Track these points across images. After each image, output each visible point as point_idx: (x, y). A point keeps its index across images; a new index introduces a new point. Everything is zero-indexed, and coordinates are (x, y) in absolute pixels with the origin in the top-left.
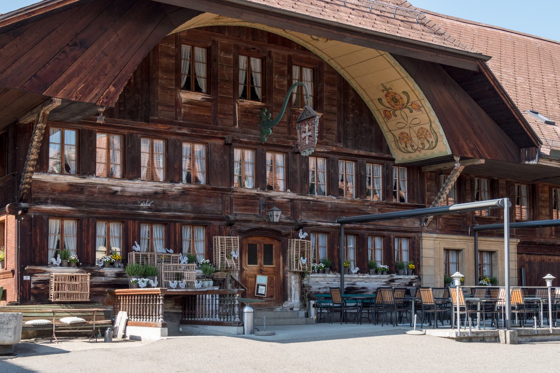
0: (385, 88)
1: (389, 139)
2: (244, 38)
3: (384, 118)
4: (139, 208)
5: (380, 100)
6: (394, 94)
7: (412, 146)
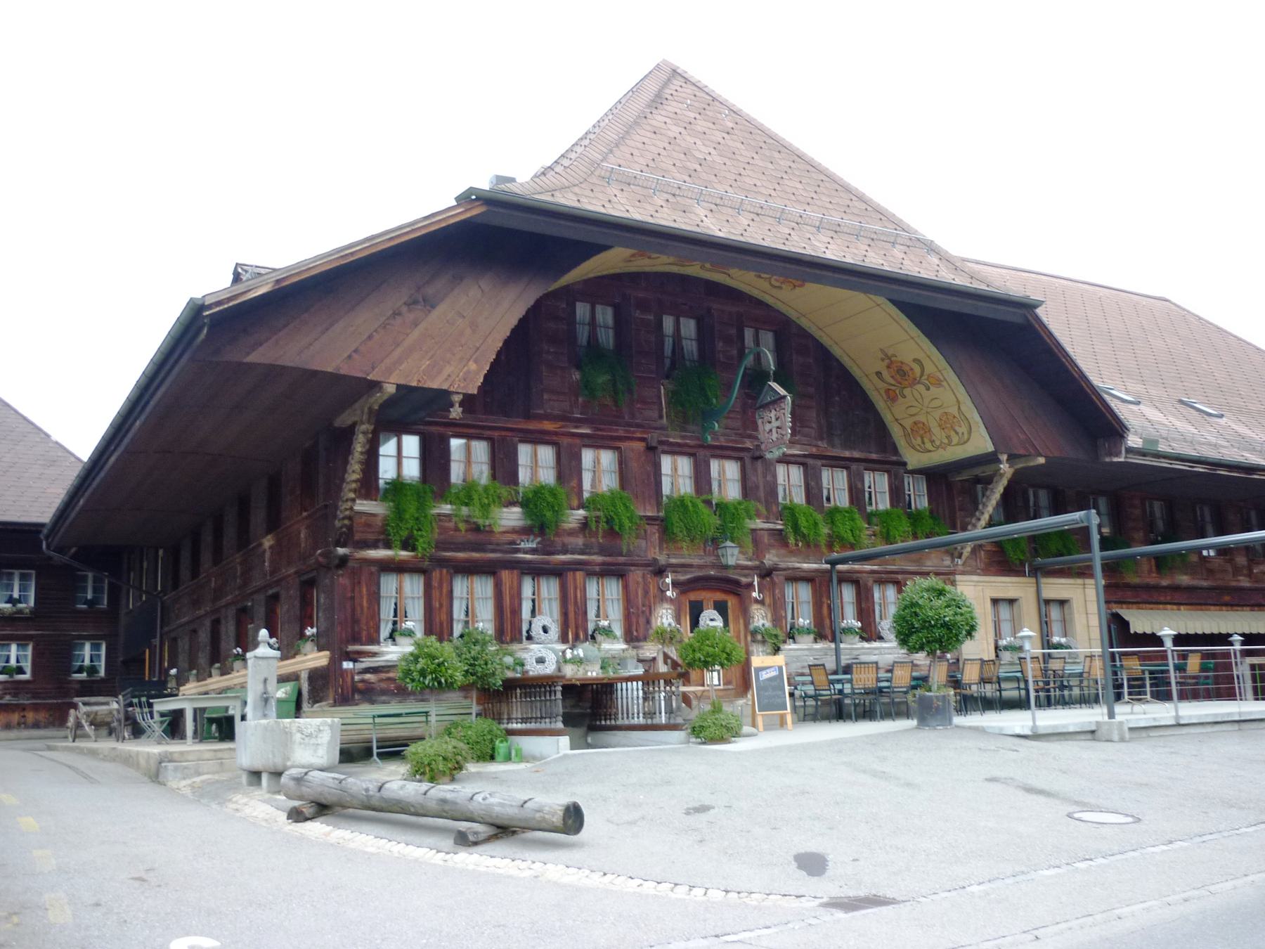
0: (886, 355)
1: (896, 432)
4: (518, 551)
5: (879, 374)
6: (899, 364)
7: (932, 442)
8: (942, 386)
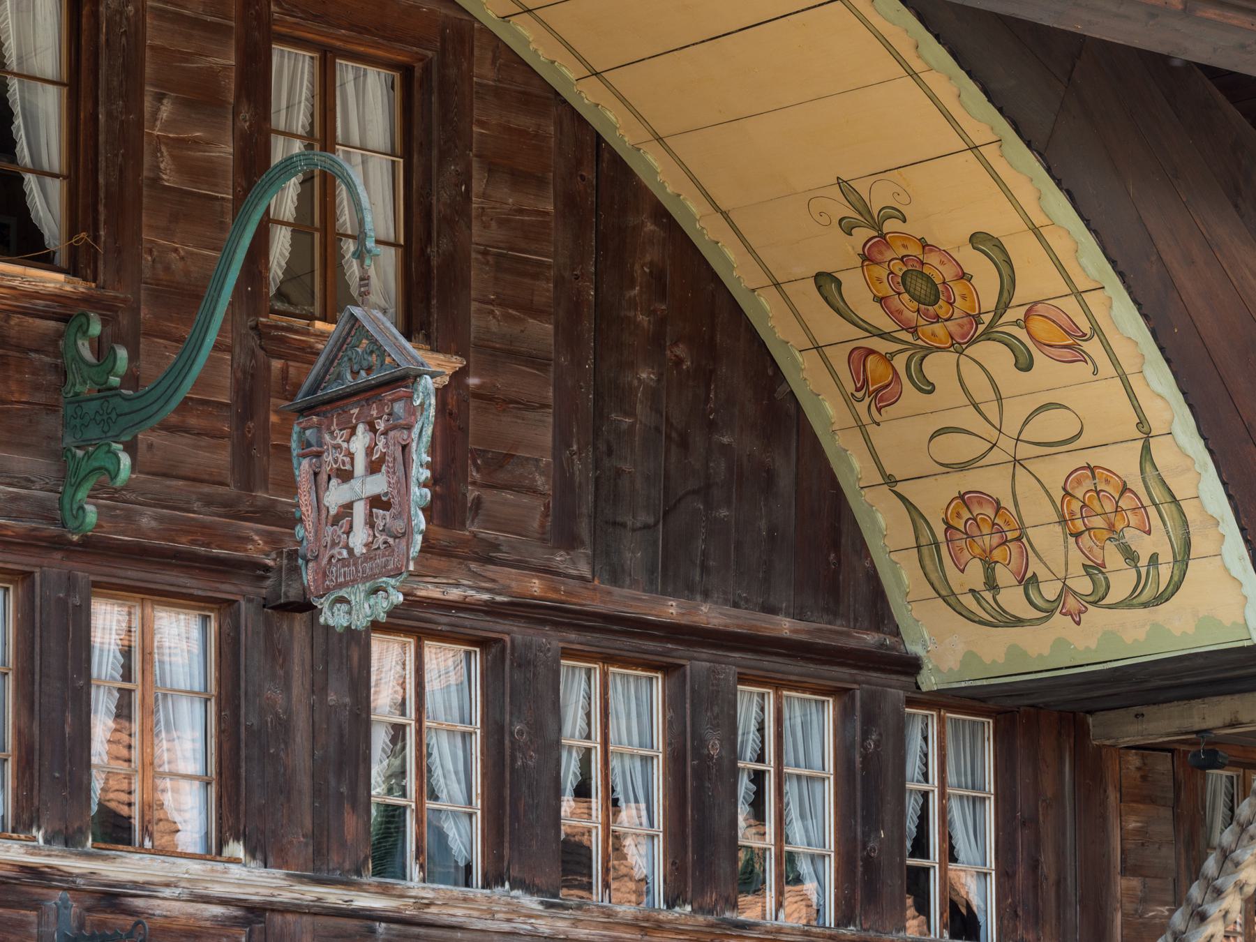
0: (863, 208)
3: (850, 400)
5: (826, 282)
6: (914, 250)
7: (1029, 582)
8: (1084, 357)
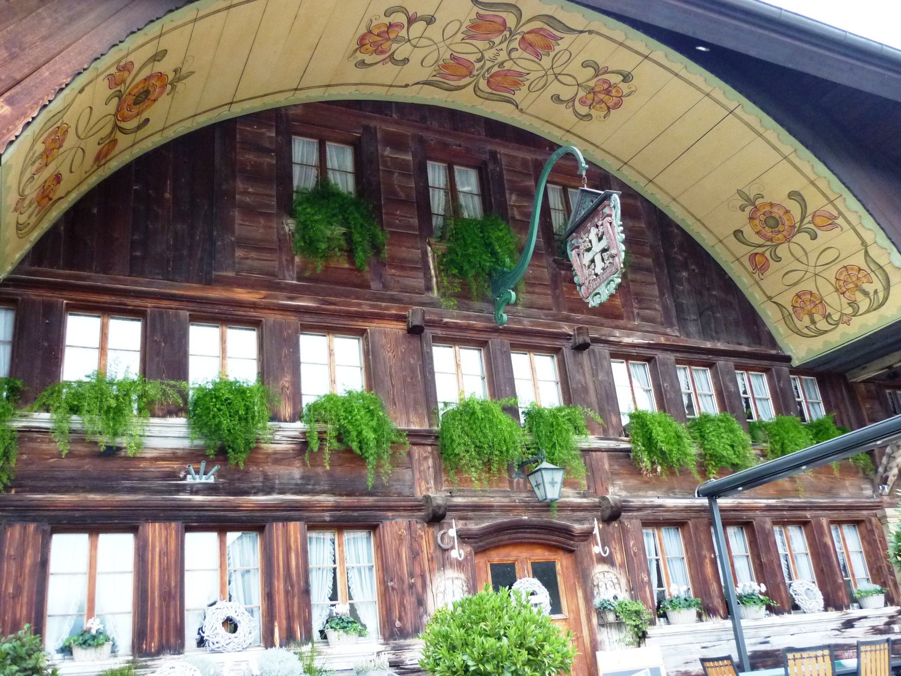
0: (748, 199)
1: (770, 316)
2: (435, 125)
3: (751, 274)
4: (181, 489)
5: (738, 233)
6: (768, 209)
7: (827, 317)
8: (836, 226)
